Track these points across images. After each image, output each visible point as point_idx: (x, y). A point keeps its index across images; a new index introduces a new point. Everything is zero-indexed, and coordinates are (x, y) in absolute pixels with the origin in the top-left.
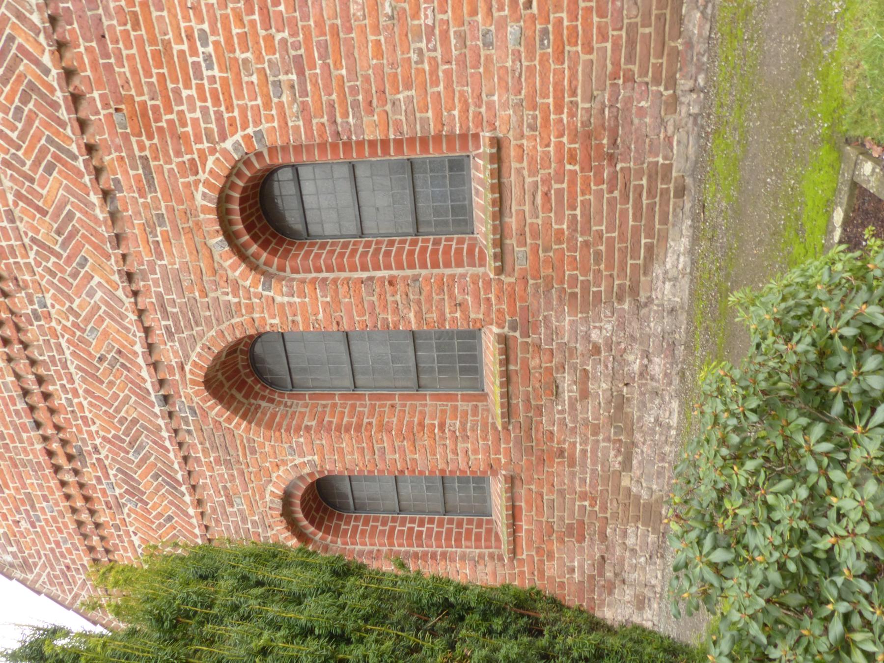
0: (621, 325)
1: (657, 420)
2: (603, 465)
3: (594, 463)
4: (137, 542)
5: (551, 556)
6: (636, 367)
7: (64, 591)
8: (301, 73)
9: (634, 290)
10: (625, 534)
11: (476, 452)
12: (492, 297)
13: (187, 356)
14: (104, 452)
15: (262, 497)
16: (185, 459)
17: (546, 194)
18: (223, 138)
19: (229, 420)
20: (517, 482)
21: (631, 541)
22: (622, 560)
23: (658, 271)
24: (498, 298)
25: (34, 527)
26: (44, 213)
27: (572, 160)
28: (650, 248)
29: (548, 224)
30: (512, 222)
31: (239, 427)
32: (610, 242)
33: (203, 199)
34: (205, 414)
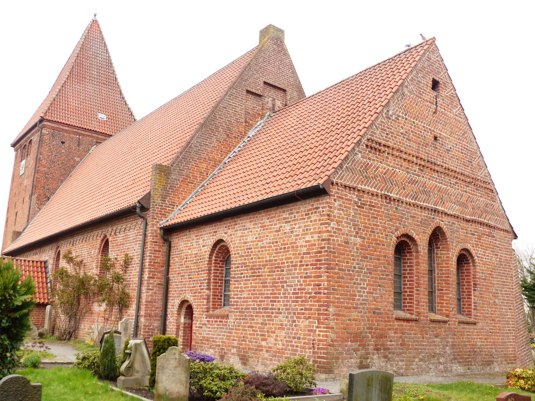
0: (449, 356)
1: (430, 368)
2: (421, 352)
3: (421, 349)
4: (398, 170)
5: (395, 333)
6: (441, 361)
7: (379, 124)
8: (485, 279)
9: (455, 359)
10: (402, 361)
11: (424, 309)
12: (454, 319)
13: (445, 224)
14: (422, 179)
15: (413, 229)
16: (421, 207)
17: (469, 335)
18: (478, 257)
19: (431, 229)
20: (416, 322)
21: (400, 363)
22: (394, 361)
23: (458, 365)
24: (454, 321)
25: (401, 133)
26: (467, 201)
27: (474, 342)
28: (460, 362)
29: (464, 335)
30: (465, 326)
31: (429, 231)
32: (461, 352)
33: (469, 246)
34: (433, 222)
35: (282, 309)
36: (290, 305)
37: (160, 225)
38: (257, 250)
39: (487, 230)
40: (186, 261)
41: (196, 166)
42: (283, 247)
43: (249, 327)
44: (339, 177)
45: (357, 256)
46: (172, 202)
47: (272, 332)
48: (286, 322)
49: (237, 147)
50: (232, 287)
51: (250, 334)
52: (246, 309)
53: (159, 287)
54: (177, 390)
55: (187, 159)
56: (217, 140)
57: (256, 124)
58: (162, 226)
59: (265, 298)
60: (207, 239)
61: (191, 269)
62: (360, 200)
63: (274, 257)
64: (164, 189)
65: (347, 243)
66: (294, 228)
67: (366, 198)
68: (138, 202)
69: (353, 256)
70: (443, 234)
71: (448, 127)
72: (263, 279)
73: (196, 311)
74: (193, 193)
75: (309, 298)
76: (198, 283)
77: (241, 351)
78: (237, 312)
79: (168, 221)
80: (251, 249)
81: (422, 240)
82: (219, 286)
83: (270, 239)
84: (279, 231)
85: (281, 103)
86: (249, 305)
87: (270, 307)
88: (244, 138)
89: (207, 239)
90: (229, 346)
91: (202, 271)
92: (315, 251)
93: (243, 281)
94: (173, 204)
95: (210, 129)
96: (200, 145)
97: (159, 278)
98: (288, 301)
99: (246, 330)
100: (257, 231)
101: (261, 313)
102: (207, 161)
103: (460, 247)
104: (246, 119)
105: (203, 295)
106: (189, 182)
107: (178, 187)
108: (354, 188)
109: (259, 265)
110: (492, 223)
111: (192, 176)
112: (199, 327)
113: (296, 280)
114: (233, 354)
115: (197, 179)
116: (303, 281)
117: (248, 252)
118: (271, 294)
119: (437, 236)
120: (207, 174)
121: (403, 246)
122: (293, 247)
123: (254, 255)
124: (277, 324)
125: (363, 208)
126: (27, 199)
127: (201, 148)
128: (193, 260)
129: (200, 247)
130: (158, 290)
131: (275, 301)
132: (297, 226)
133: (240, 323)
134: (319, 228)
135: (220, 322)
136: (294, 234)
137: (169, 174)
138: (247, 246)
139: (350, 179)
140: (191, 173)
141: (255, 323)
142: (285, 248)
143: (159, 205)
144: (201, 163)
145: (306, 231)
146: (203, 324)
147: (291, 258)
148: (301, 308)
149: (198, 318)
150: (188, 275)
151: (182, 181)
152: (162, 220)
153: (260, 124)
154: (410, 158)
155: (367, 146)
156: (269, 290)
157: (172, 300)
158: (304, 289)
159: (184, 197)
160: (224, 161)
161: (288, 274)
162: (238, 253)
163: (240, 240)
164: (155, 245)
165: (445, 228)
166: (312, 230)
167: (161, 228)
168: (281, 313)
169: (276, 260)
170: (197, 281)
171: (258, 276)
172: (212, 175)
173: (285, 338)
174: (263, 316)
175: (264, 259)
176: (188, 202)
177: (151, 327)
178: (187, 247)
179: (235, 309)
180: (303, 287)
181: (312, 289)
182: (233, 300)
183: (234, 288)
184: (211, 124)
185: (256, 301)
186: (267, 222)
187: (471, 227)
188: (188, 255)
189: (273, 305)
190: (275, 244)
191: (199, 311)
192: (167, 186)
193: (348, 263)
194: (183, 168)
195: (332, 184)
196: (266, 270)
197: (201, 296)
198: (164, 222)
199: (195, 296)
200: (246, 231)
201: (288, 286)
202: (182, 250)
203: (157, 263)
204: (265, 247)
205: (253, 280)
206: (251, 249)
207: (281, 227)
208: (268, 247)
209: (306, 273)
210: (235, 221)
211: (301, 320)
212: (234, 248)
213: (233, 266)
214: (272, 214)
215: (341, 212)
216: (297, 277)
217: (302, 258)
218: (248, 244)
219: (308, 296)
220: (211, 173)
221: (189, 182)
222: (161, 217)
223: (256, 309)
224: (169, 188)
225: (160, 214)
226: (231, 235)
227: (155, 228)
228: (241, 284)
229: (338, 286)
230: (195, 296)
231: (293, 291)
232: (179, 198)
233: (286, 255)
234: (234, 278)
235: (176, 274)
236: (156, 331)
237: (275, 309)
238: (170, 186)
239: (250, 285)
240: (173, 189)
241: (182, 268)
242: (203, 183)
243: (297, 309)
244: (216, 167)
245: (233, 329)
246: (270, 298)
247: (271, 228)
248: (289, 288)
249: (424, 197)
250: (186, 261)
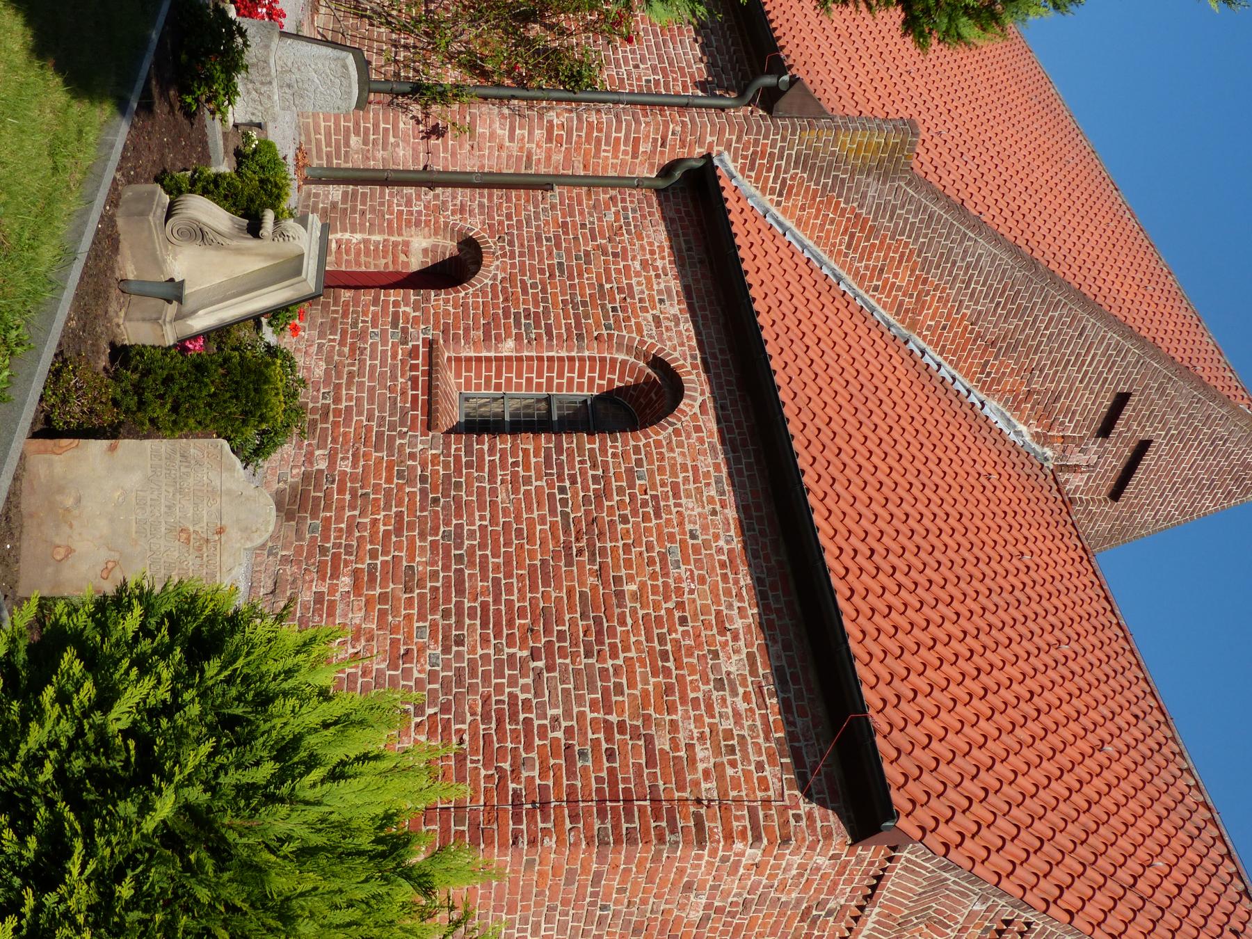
35: (459, 656)
36: (472, 689)
37: (719, 154)
38: (653, 539)
40: (605, 253)
41: (903, 254)
42: (669, 647)
43: (399, 515)
44: (915, 864)
45: (642, 913)
46: (791, 187)
47: (382, 613)
48: (416, 674)
49: (954, 372)
51: (375, 522)
52: (457, 500)
53: (519, 159)
54: (80, 546)
55: (928, 227)
56: (980, 313)
57: (1020, 419)
58: (716, 162)
59: (496, 581)
60: (679, 333)
61: (580, 275)
62: (829, 913)
63: (634, 611)
65: (688, 887)
66: (734, 693)
68: (794, 80)
69: (644, 902)
72: (557, 568)
73: (447, 301)
74: (819, 250)
75: (498, 769)
76: (536, 305)
77: (317, 487)
78: (446, 465)
79: (732, 177)
80: (658, 516)
82: (529, 380)
83: (691, 592)
84: (723, 630)
85: (1078, 487)
86: (471, 515)
87: (467, 605)
88: (982, 390)
89: (679, 333)
90: (334, 441)
91: (577, 316)
92: (661, 783)
93: (550, 485)
94: (784, 191)
95: (1019, 291)
96: (968, 266)
97: (548, 158)
98: (486, 676)
99: (387, 507)
100: (716, 537)
101: (446, 568)
102: (916, 286)
104: (1039, 393)
105: (497, 327)
106: (852, 236)
107: (838, 203)
108: (871, 896)
109: (603, 551)
111: (873, 245)
112: (396, 315)
113: (559, 711)
114: (309, 458)
115: (860, 261)
116: (555, 741)
117: (645, 504)
118: (509, 603)
120: (876, 289)
122: (669, 690)
123: (636, 524)
124: (409, 637)
125: (802, 920)
127: (960, 268)
128: (609, 280)
129: (654, 308)
130: (509, 157)
131: (484, 625)
132: (742, 706)
133: (410, 482)
134: (738, 800)
135: (415, 398)
136: (715, 694)
137: (885, 176)
138: (667, 499)
139: (905, 888)
140: (882, 243)
141: (411, 541)
142: (664, 656)
143: (782, 148)
144: (913, 271)
145: (726, 745)
146: (405, 330)
147: (632, 685)
148: (466, 737)
149: (425, 311)
150: (560, 264)
151: (857, 216)
152: (735, 161)
153: (1018, 433)
155: (1008, 923)
156: (522, 598)
157: (481, 205)
158: (529, 747)
159: (807, 224)
160: (915, 336)
161: (577, 673)
162: (639, 463)
163: (684, 468)
164: (655, 140)
166: (730, 771)
167: (708, 157)
168: (446, 650)
169: (623, 622)
170: (545, 300)
171: (568, 547)
172: (873, 302)
173: (364, 674)
174: (434, 576)
175: (623, 572)
176: (789, 237)
177: (392, 140)
178: (652, 252)
179: (457, 458)
180: (537, 742)
181: (530, 780)
182: (486, 447)
183: (526, 451)
184: (1033, 294)
185: (483, 546)
188: (625, 259)
189: (472, 616)
190: (677, 614)
191: (447, 313)
192: (845, 171)
193: (621, 891)
194: (900, 216)
195: (894, 849)
196: (591, 580)
197: (495, 316)
198: (727, 164)
199: (495, 296)
200: (713, 493)
201: (539, 675)
202: (640, 238)
203: (598, 150)
204: (666, 575)
205: (553, 524)
206: (658, 516)
207: (736, 638)
208: (665, 584)
209: (582, 754)
210: (744, 444)
211: (423, 738)
212: (658, 444)
213: (596, 446)
214: (777, 599)
215: (794, 872)
216: (568, 714)
217: (635, 735)
218: (671, 502)
219: (507, 766)
220: (879, 300)
221: (852, 236)
222: (745, 157)
223: (459, 547)
224: (836, 177)
225: (755, 153)
226: (698, 429)
227: (709, 139)
228: (538, 478)
229: (540, 874)
230: (495, 296)
231: (522, 696)
232: (803, 208)
233: (642, 661)
234: (559, 450)
235: (564, 216)
236: (380, 154)
237: (459, 624)
238: (843, 180)
239: (535, 515)
240: (833, 190)
241: (584, 235)
242: (849, 279)
243: (460, 718)
244: (897, 314)
245: (390, 454)
246: (497, 601)
247: (728, 593)
248: (529, 681)
250: (605, 253)
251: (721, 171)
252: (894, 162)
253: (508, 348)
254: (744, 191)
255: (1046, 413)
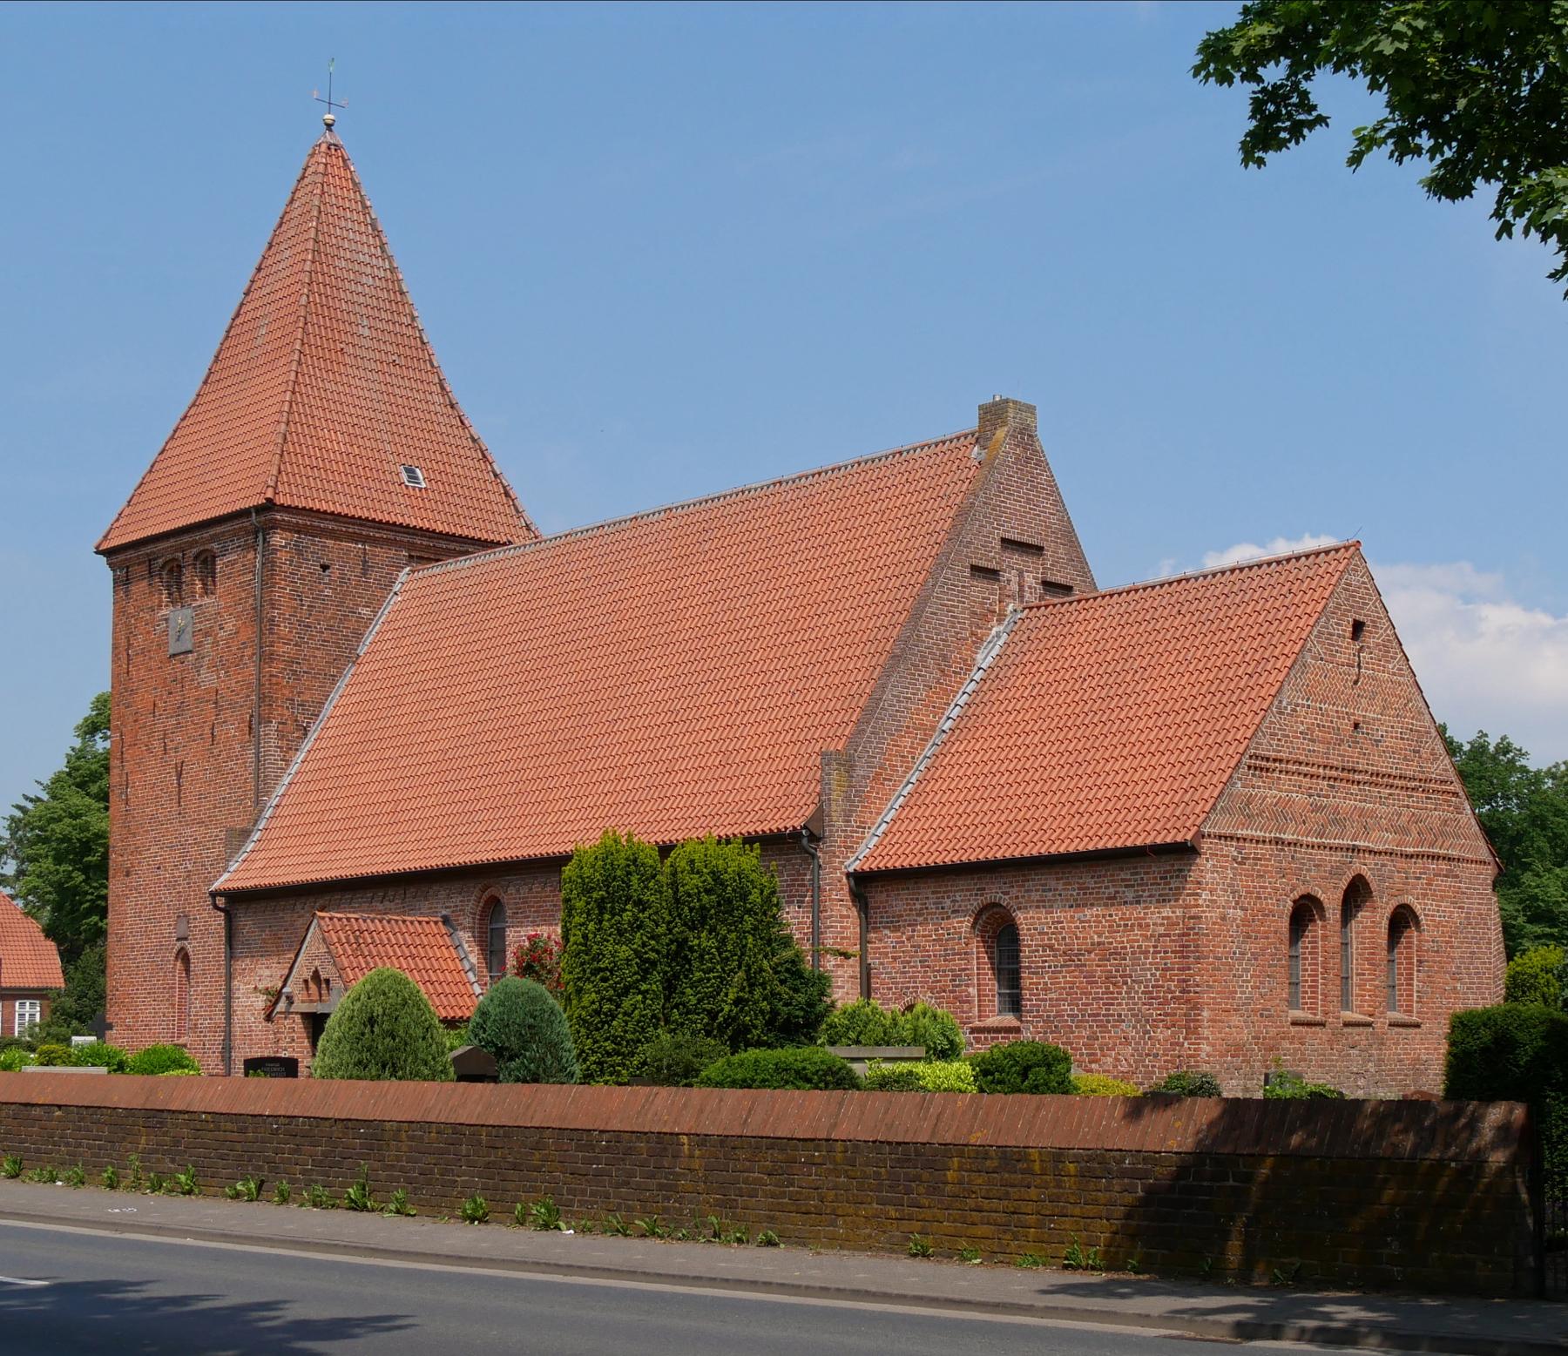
31: (1344, 885)
33: (1409, 899)
39: (1444, 866)
50: (1025, 983)
58: (851, 870)
64: (847, 798)
65: (1223, 918)
67: (1249, 848)
68: (805, 827)
70: (1366, 884)
71: (1378, 700)
81: (1331, 900)
94: (862, 826)
103: (1394, 903)
110: (1454, 853)
119: (1356, 894)
121: (1304, 912)
122: (1140, 925)
126: (232, 730)
153: (998, 636)
154: (1314, 770)
165: (1368, 875)
167: (848, 875)
186: (1091, 883)
187: (1415, 867)
217: (1158, 941)
249: (1335, 830)
251: (856, 866)
252: (847, 764)
253: (973, 991)
254: (867, 850)
255: (985, 616)
